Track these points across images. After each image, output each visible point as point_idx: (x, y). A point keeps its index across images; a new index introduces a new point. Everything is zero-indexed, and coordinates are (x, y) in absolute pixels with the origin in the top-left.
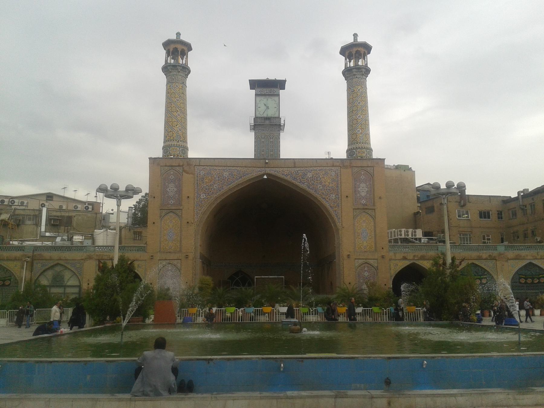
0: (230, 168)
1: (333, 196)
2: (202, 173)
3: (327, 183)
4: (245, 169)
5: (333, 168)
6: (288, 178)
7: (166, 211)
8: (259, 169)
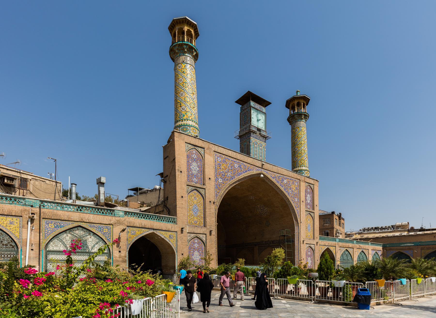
0: (239, 161)
1: (296, 200)
2: (220, 160)
3: (293, 190)
4: (249, 165)
5: (296, 180)
6: (274, 180)
7: (191, 187)
8: (257, 168)
